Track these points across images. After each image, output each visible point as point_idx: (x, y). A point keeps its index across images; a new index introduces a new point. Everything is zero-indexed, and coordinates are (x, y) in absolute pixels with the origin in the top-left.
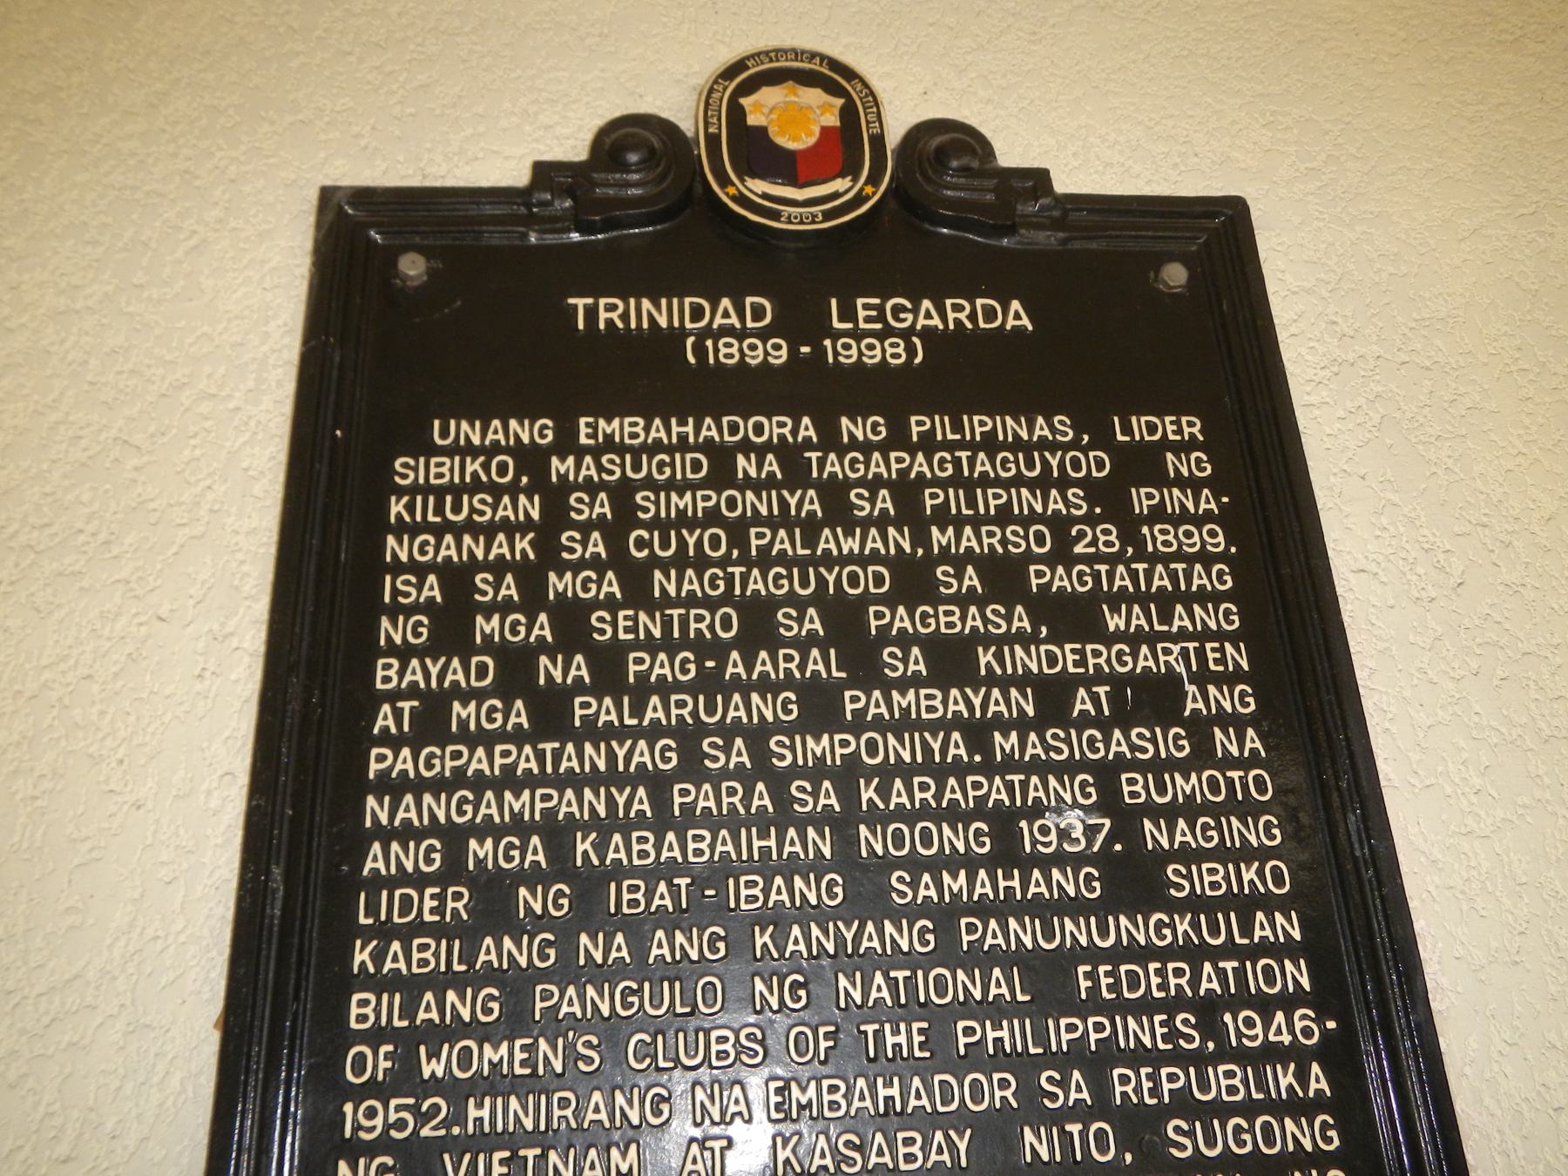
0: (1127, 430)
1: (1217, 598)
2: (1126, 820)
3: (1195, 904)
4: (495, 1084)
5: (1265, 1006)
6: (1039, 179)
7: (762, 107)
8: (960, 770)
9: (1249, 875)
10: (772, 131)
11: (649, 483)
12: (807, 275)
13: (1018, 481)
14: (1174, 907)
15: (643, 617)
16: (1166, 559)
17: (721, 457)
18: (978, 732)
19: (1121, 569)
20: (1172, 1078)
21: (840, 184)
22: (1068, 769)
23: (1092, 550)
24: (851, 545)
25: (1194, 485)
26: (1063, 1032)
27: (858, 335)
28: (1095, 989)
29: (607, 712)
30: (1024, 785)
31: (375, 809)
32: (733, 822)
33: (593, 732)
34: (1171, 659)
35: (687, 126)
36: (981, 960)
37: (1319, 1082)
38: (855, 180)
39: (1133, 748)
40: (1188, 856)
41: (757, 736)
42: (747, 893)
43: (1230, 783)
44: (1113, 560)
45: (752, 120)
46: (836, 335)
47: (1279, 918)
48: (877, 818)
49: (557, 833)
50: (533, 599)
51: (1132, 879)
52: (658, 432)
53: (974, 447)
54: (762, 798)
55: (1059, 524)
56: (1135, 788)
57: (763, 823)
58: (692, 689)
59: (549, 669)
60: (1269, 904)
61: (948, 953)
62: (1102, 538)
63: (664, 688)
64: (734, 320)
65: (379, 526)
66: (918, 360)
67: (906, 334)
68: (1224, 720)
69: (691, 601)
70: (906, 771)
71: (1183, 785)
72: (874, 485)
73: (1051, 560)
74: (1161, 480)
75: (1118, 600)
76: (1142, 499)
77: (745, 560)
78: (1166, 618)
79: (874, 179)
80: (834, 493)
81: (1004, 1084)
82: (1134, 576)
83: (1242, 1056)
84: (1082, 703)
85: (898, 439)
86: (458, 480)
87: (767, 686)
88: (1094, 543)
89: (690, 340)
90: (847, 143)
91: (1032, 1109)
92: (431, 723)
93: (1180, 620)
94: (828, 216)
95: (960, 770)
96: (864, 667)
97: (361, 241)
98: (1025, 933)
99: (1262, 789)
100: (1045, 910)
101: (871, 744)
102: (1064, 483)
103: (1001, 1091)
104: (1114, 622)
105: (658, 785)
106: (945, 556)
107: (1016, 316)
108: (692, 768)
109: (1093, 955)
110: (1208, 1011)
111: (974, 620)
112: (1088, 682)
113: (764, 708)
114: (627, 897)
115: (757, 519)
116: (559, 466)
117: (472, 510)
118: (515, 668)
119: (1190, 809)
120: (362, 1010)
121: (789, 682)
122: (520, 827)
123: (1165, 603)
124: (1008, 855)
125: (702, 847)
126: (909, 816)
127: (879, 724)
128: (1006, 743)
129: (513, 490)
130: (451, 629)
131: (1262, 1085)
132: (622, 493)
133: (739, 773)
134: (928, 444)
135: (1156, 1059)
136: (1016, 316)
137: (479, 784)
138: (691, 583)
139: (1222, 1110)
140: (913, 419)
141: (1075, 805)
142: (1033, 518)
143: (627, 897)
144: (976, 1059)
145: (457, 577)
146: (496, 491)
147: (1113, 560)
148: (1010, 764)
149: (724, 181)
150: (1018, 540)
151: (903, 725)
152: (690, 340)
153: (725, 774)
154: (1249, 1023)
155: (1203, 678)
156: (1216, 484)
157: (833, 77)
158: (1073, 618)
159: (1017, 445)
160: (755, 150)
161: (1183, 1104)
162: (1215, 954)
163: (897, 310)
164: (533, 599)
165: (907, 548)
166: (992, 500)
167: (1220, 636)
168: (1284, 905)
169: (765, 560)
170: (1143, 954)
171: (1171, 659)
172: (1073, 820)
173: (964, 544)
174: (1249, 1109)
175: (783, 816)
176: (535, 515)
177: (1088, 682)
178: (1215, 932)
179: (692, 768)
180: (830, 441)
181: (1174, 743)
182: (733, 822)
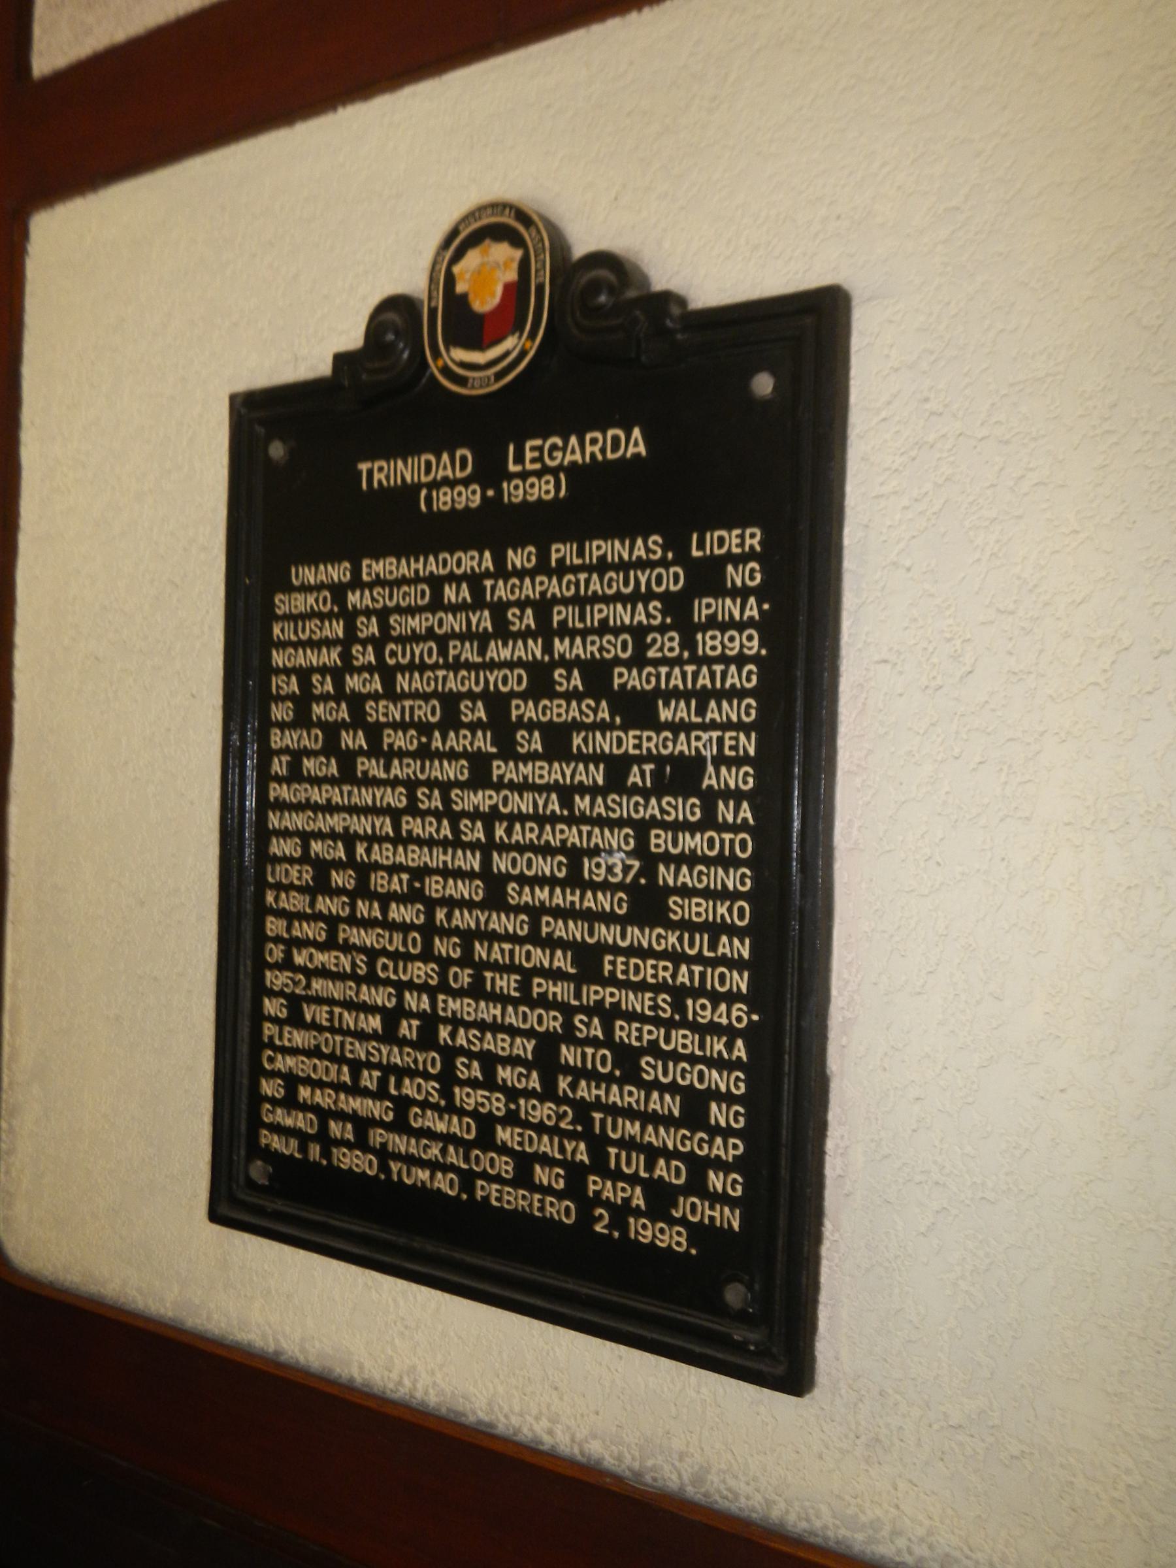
0: (701, 545)
1: (741, 694)
2: (649, 860)
3: (686, 926)
5: (716, 998)
8: (553, 819)
9: (722, 910)
10: (471, 297)
11: (398, 610)
12: (490, 427)
13: (619, 597)
14: (670, 925)
15: (391, 706)
16: (709, 661)
17: (436, 583)
18: (567, 794)
19: (677, 670)
20: (650, 1032)
21: (510, 343)
22: (620, 823)
23: (659, 655)
24: (505, 654)
25: (742, 593)
26: (593, 993)
27: (524, 475)
28: (613, 973)
30: (590, 834)
32: (430, 843)
33: (369, 781)
34: (700, 744)
36: (551, 943)
37: (740, 1050)
38: (520, 337)
39: (662, 811)
40: (686, 892)
41: (445, 787)
42: (434, 887)
43: (722, 841)
44: (671, 663)
45: (460, 288)
46: (511, 477)
47: (736, 942)
48: (503, 848)
49: (349, 839)
51: (648, 904)
52: (404, 570)
53: (589, 569)
54: (446, 831)
55: (639, 633)
56: (659, 841)
57: (444, 844)
58: (413, 755)
60: (732, 931)
61: (535, 938)
62: (668, 644)
63: (401, 754)
64: (449, 473)
65: (269, 643)
66: (563, 493)
67: (554, 471)
68: (727, 794)
69: (415, 695)
70: (522, 818)
72: (522, 604)
73: (629, 664)
74: (719, 589)
75: (671, 695)
76: (704, 607)
77: (447, 666)
78: (701, 711)
79: (532, 336)
80: (499, 610)
81: (555, 1018)
82: (684, 675)
83: (695, 1027)
84: (634, 778)
85: (542, 567)
87: (452, 755)
88: (661, 649)
89: (424, 492)
91: (569, 1035)
93: (712, 714)
94: (499, 376)
95: (553, 819)
98: (575, 931)
99: (743, 848)
100: (591, 917)
101: (506, 799)
102: (650, 596)
103: (553, 1022)
104: (665, 714)
105: (395, 815)
106: (563, 662)
107: (636, 444)
108: (413, 809)
109: (615, 950)
110: (679, 994)
111: (574, 713)
112: (640, 760)
114: (379, 882)
115: (453, 635)
116: (353, 598)
117: (311, 631)
119: (691, 859)
121: (465, 754)
122: (333, 835)
123: (703, 697)
124: (575, 880)
125: (416, 857)
126: (520, 848)
127: (512, 786)
128: (582, 804)
129: (330, 616)
131: (702, 1046)
132: (383, 615)
133: (436, 814)
134: (562, 569)
135: (642, 1019)
136: (636, 444)
137: (316, 808)
138: (417, 685)
139: (675, 1056)
140: (554, 547)
141: (620, 849)
142: (624, 629)
144: (544, 1002)
145: (304, 675)
146: (322, 616)
147: (671, 663)
148: (584, 819)
149: (436, 354)
150: (616, 647)
151: (522, 787)
152: (424, 492)
153: (429, 812)
154: (703, 1007)
155: (720, 760)
156: (761, 593)
158: (637, 710)
159: (623, 567)
161: (653, 1049)
162: (690, 960)
163: (554, 447)
164: (340, 694)
165: (538, 655)
167: (740, 726)
168: (739, 932)
169: (456, 666)
170: (645, 953)
171: (700, 744)
172: (615, 858)
173: (575, 651)
174: (693, 1059)
175: (456, 843)
176: (341, 634)
177: (640, 760)
178: (691, 945)
180: (502, 571)
181: (689, 809)
182: (430, 843)
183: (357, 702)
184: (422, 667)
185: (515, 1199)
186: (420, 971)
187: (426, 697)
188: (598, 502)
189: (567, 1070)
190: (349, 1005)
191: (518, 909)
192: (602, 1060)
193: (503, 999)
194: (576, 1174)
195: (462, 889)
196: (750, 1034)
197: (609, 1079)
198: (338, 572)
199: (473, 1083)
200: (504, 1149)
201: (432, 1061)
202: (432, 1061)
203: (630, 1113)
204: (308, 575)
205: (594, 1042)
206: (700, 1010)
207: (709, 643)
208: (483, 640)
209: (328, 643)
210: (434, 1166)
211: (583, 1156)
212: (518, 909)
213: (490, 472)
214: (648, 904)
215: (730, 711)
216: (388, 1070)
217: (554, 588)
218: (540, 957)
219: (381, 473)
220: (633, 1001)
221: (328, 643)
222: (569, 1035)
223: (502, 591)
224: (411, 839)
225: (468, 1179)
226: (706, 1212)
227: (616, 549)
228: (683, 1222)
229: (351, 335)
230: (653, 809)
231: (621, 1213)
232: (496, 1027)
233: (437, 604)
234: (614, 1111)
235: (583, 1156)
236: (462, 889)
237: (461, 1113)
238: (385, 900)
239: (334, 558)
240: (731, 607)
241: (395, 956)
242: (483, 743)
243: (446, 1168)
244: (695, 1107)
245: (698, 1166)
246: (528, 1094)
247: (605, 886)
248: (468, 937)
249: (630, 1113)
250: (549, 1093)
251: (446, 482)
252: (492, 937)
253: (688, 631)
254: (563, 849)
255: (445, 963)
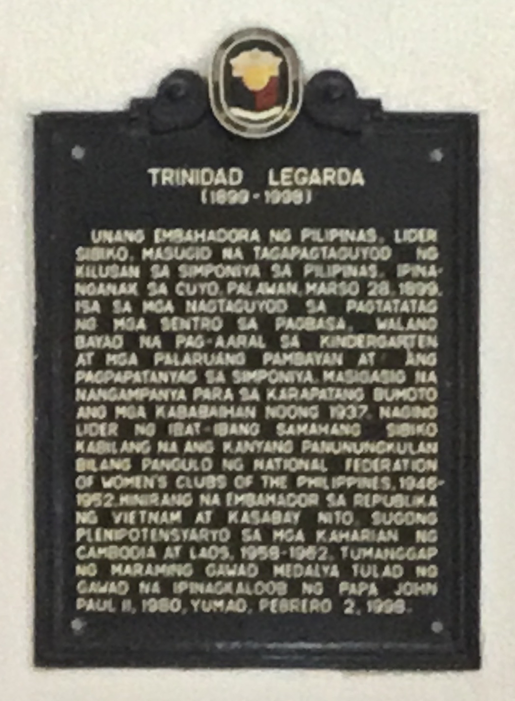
3: (397, 439)
5: (418, 476)
8: (309, 386)
11: (185, 261)
13: (348, 262)
16: (409, 298)
17: (217, 249)
18: (318, 371)
21: (276, 111)
24: (271, 291)
25: (427, 263)
26: (338, 481)
32: (216, 403)
33: (162, 367)
36: (310, 456)
38: (284, 107)
40: (398, 421)
41: (228, 370)
42: (221, 430)
44: (385, 298)
45: (236, 74)
48: (274, 403)
49: (150, 405)
51: (374, 429)
53: (329, 244)
54: (229, 395)
55: (364, 283)
57: (228, 404)
58: (202, 351)
60: (427, 440)
61: (297, 453)
63: (191, 350)
67: (304, 188)
68: (422, 368)
69: (202, 314)
74: (412, 259)
75: (385, 316)
80: (266, 266)
83: (405, 492)
84: (363, 360)
85: (296, 240)
87: (232, 351)
91: (323, 506)
95: (309, 386)
100: (336, 439)
102: (368, 262)
103: (313, 500)
104: (381, 326)
109: (353, 456)
110: (395, 477)
112: (367, 351)
114: (176, 430)
119: (401, 403)
121: (241, 349)
122: (135, 403)
123: (405, 318)
125: (205, 412)
126: (286, 403)
127: (278, 368)
132: (174, 265)
135: (372, 492)
136: (358, 178)
144: (306, 489)
145: (106, 302)
146: (120, 264)
147: (385, 298)
148: (329, 384)
150: (346, 289)
156: (438, 263)
158: (363, 324)
161: (380, 507)
162: (401, 457)
164: (137, 312)
167: (427, 333)
169: (234, 297)
175: (237, 402)
177: (367, 351)
180: (265, 241)
181: (399, 376)
182: (216, 403)
184: (207, 298)
185: (289, 606)
186: (211, 481)
187: (211, 316)
188: (329, 208)
189: (323, 526)
190: (153, 509)
191: (285, 438)
192: (346, 518)
193: (277, 491)
194: (331, 586)
196: (438, 492)
197: (350, 528)
199: (256, 544)
200: (279, 578)
201: (225, 534)
202: (225, 534)
203: (366, 545)
205: (341, 509)
208: (254, 283)
209: (128, 281)
210: (227, 597)
211: (335, 573)
212: (285, 438)
216: (186, 546)
217: (304, 254)
218: (302, 464)
221: (128, 281)
222: (323, 506)
224: (200, 402)
225: (252, 601)
227: (346, 235)
228: (402, 596)
230: (375, 377)
231: (361, 601)
232: (271, 508)
233: (217, 258)
234: (355, 545)
235: (335, 573)
237: (247, 562)
238: (181, 441)
240: (419, 270)
241: (192, 474)
243: (235, 598)
244: (407, 535)
245: (410, 568)
246: (296, 544)
247: (345, 421)
248: (248, 459)
249: (366, 545)
250: (310, 540)
251: (221, 186)
252: (266, 456)
253: (394, 281)
254: (315, 401)
255: (231, 475)
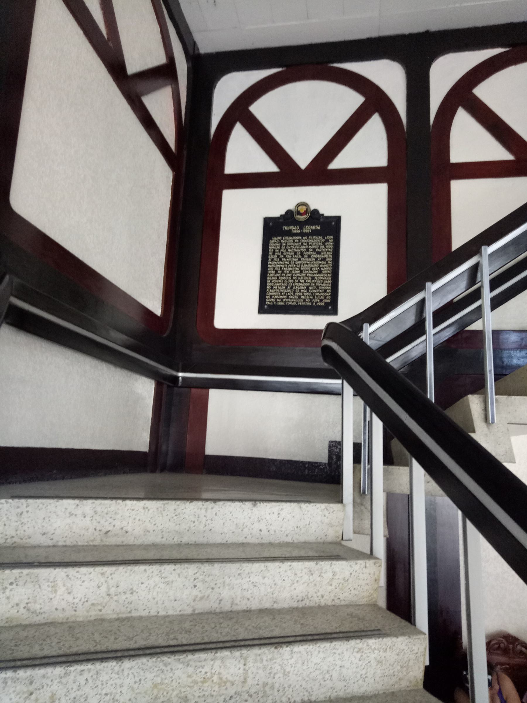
4: (276, 283)
6: (323, 215)
7: (300, 208)
12: (302, 224)
18: (311, 262)
26: (313, 281)
29: (284, 260)
31: (269, 266)
35: (294, 210)
41: (295, 262)
42: (293, 272)
49: (281, 268)
50: (279, 251)
51: (320, 272)
55: (319, 246)
56: (321, 266)
59: (281, 257)
71: (324, 266)
86: (274, 241)
90: (306, 212)
92: (272, 260)
96: (303, 256)
97: (267, 221)
100: (313, 274)
103: (309, 285)
107: (319, 228)
110: (324, 281)
113: (295, 260)
118: (278, 257)
120: (268, 278)
125: (290, 269)
130: (274, 254)
136: (319, 228)
143: (285, 272)
157: (305, 204)
158: (319, 253)
160: (299, 213)
166: (314, 244)
179: (290, 263)
181: (325, 262)
183: (282, 253)
185: (304, 304)
186: (291, 281)
188: (314, 233)
192: (315, 288)
194: (311, 300)
195: (297, 272)
198: (280, 238)
201: (293, 291)
204: (275, 238)
206: (326, 281)
207: (327, 247)
211: (312, 297)
213: (301, 228)
214: (320, 272)
215: (329, 253)
218: (307, 278)
219: (286, 228)
220: (318, 281)
223: (303, 241)
226: (326, 301)
227: (317, 237)
229: (283, 212)
231: (316, 303)
236: (297, 272)
239: (280, 236)
242: (300, 256)
244: (325, 291)
248: (297, 277)
250: (308, 292)
